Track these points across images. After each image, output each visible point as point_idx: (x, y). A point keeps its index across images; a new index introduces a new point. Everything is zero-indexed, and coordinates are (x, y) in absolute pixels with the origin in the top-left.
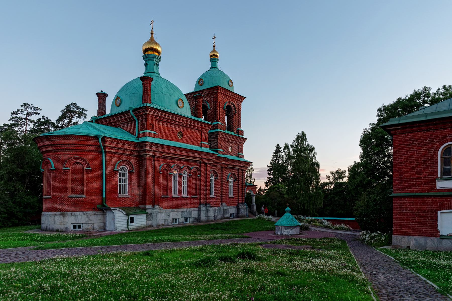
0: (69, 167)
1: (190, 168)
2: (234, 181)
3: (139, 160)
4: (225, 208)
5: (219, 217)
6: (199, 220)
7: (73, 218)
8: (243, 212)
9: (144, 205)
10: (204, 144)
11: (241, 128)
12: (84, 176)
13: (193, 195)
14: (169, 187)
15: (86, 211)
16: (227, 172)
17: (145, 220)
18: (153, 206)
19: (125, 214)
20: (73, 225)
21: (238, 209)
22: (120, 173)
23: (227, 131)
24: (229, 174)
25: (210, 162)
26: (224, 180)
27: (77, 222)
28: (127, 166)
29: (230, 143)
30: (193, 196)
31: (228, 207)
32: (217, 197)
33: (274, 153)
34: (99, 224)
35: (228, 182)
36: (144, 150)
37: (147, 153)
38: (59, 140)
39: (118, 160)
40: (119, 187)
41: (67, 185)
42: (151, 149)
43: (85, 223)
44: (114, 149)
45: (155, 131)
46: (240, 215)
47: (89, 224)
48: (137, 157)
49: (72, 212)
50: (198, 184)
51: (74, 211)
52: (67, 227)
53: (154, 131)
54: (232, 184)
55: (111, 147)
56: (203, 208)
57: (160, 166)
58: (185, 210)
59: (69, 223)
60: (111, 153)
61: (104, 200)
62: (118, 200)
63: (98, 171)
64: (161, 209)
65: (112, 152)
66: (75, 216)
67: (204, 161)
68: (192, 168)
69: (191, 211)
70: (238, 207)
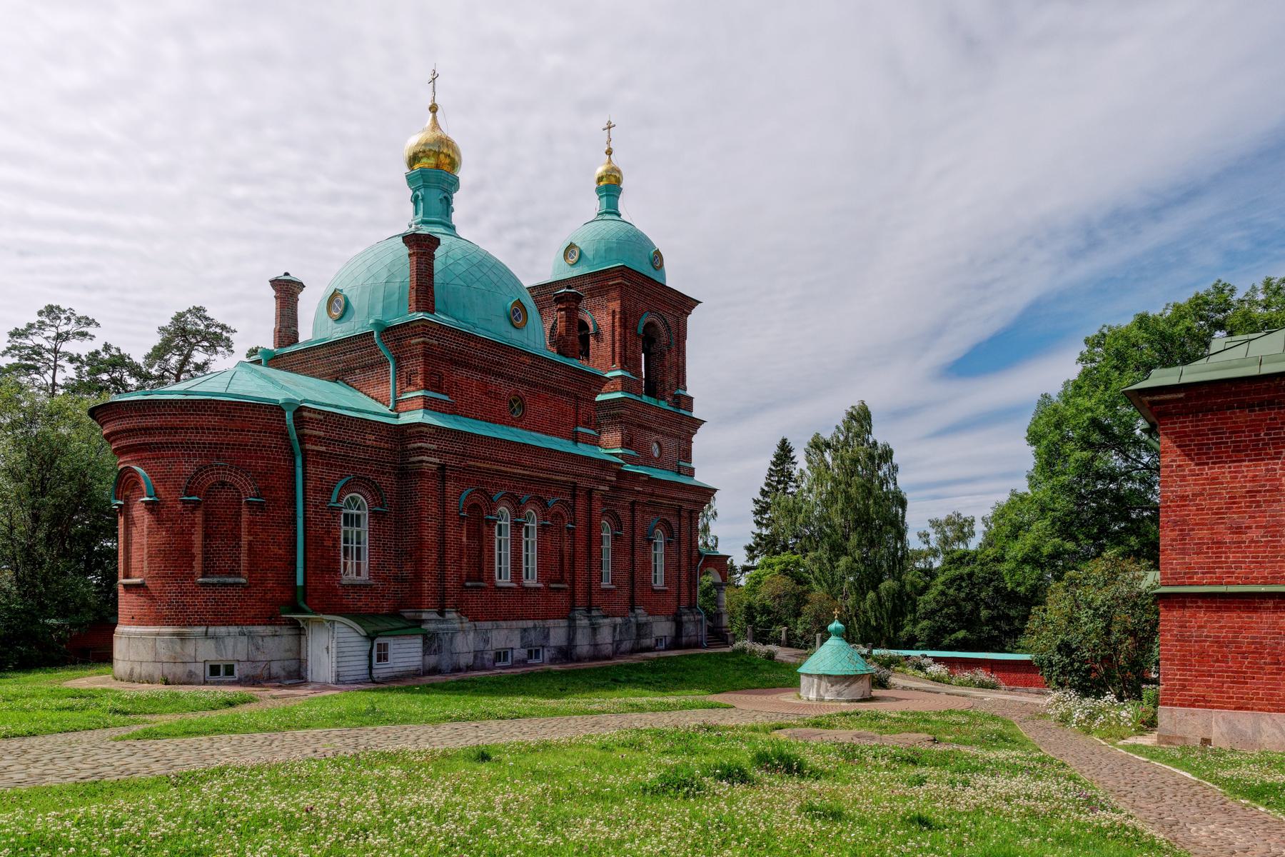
0: (199, 496)
1: (546, 504)
2: (668, 543)
3: (399, 478)
4: (643, 619)
5: (627, 645)
6: (571, 653)
7: (210, 644)
8: (693, 633)
9: (415, 608)
10: (584, 434)
11: (685, 389)
12: (240, 522)
13: (553, 583)
14: (486, 557)
15: (247, 625)
16: (646, 516)
17: (421, 654)
18: (441, 613)
19: (363, 632)
20: (212, 667)
21: (679, 626)
22: (346, 516)
23: (645, 399)
24: (655, 523)
25: (602, 488)
26: (638, 539)
27: (222, 656)
28: (369, 497)
29: (657, 432)
30: (552, 586)
31: (650, 618)
32: (619, 587)
33: (773, 463)
34: (287, 663)
35: (649, 544)
36: (414, 449)
37: (425, 458)
38: (169, 414)
39: (341, 477)
40: (342, 554)
41: (192, 547)
42: (435, 447)
43: (245, 659)
44: (330, 443)
45: (446, 394)
46: (684, 640)
47: (259, 664)
48: (394, 468)
49: (208, 626)
50: (566, 546)
51: (214, 625)
52: (193, 669)
53: (442, 393)
54: (660, 551)
56: (581, 620)
57: (459, 496)
58: (530, 624)
59: (198, 660)
61: (300, 594)
62: (340, 593)
63: (283, 507)
64: (465, 619)
65: (322, 452)
66: (215, 637)
67: (583, 484)
68: (551, 502)
69: (549, 628)
70: (678, 618)
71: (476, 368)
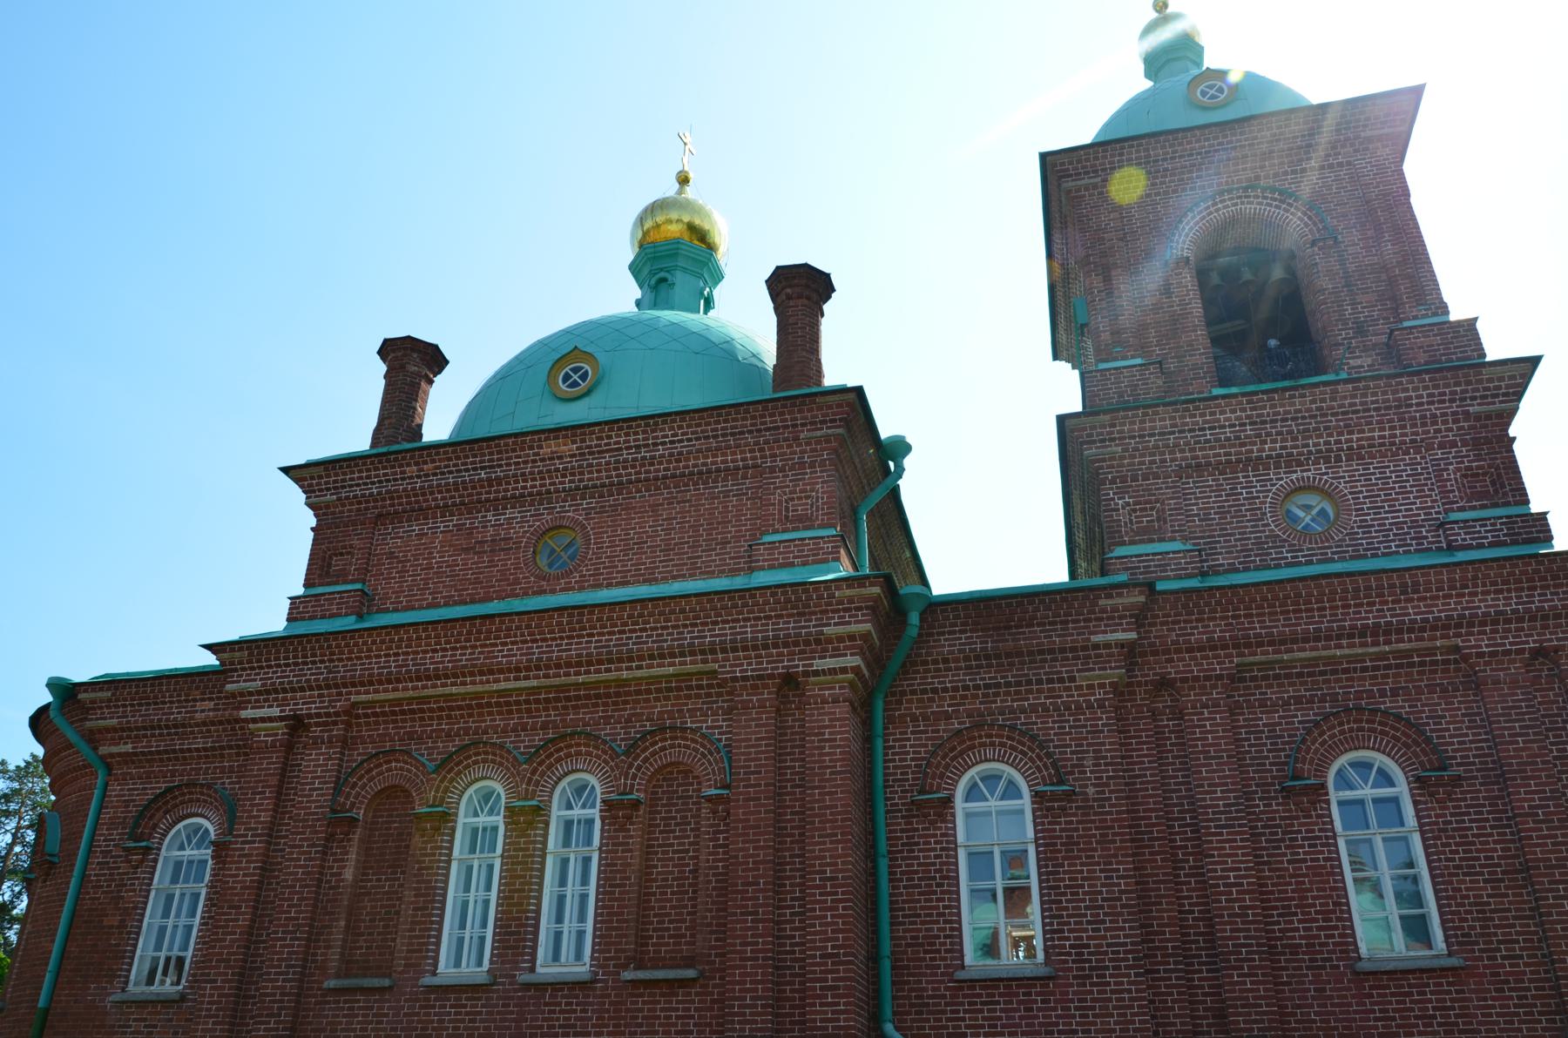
55: (115, 730)
60: (127, 758)
65: (127, 754)
71: (446, 509)
